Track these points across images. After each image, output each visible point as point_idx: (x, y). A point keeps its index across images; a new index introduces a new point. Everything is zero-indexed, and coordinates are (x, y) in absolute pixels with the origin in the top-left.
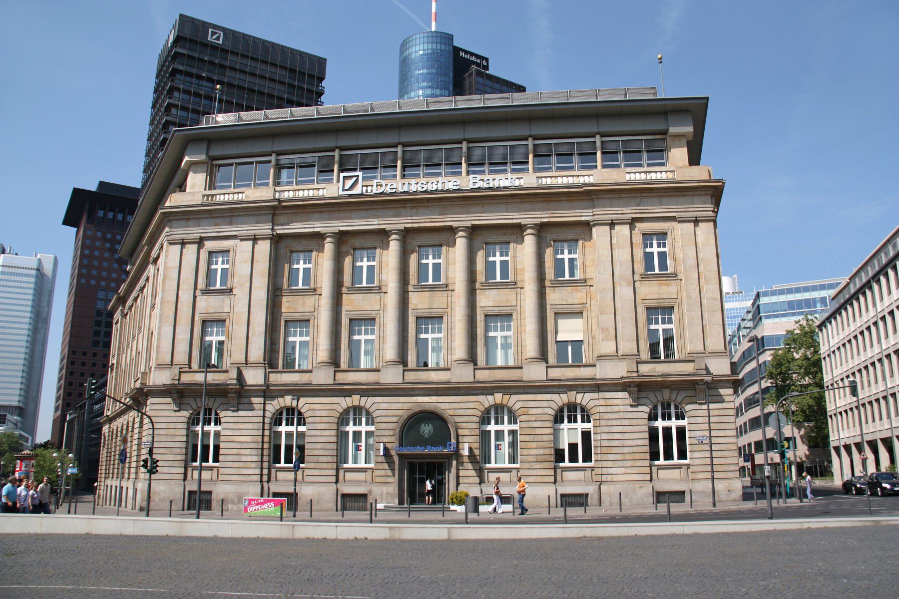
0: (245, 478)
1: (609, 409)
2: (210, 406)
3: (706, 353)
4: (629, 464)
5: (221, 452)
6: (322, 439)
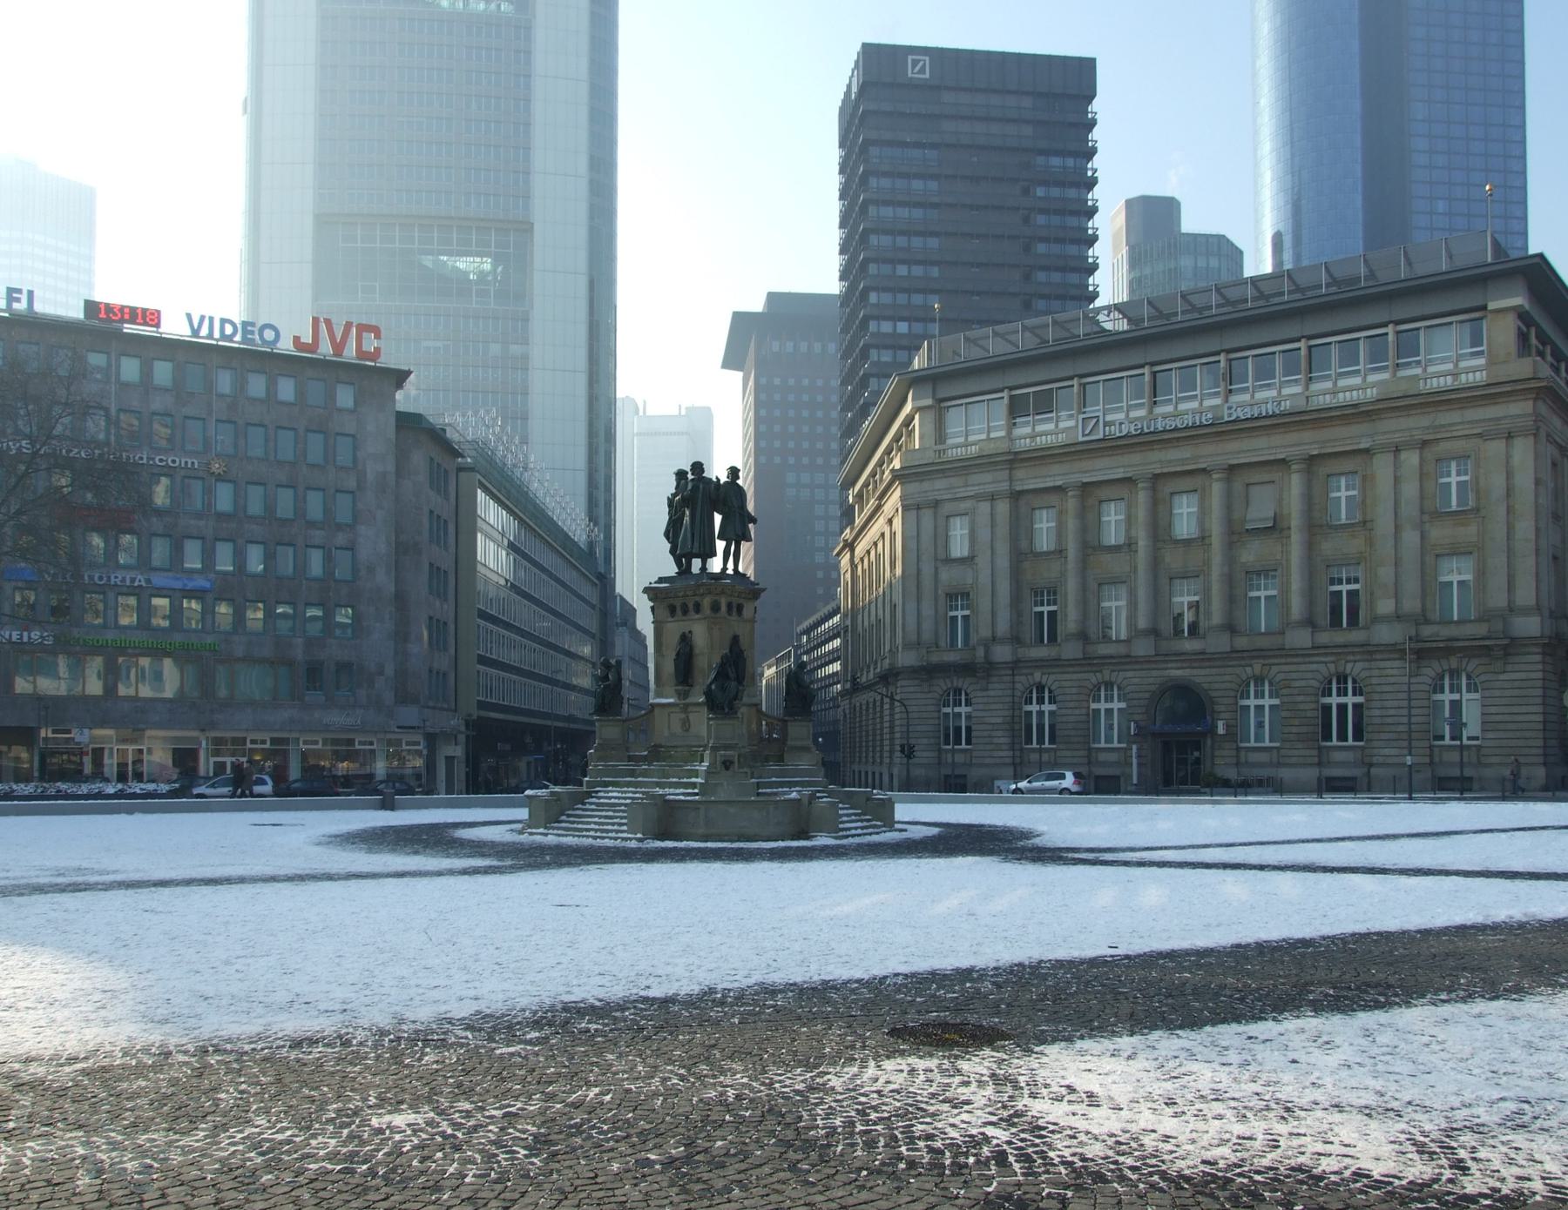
0: (998, 761)
1: (1383, 680)
2: (960, 686)
5: (974, 734)
6: (1072, 719)
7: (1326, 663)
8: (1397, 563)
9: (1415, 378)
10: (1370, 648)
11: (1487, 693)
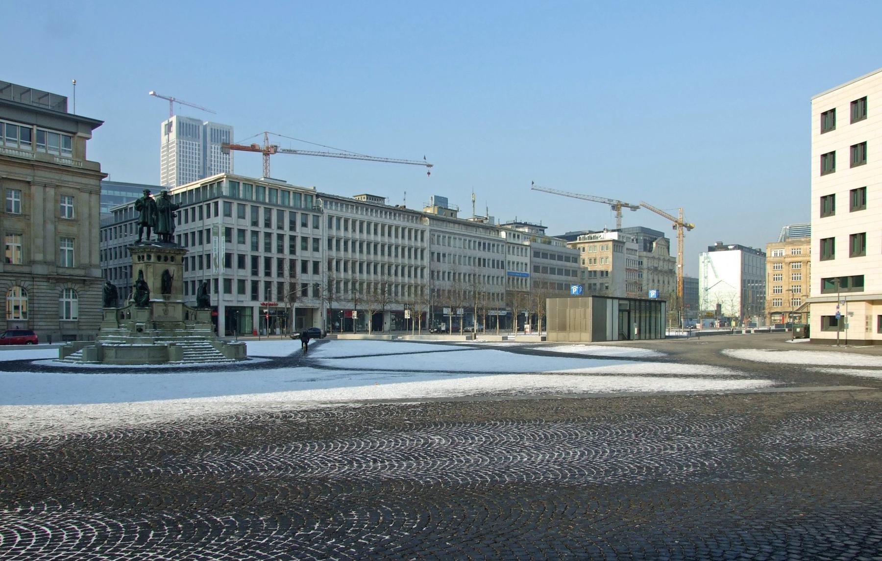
1: (39, 291)
3: (91, 266)
4: (48, 320)
7: (10, 280)
8: (44, 238)
9: (53, 156)
10: (33, 276)
11: (82, 299)
